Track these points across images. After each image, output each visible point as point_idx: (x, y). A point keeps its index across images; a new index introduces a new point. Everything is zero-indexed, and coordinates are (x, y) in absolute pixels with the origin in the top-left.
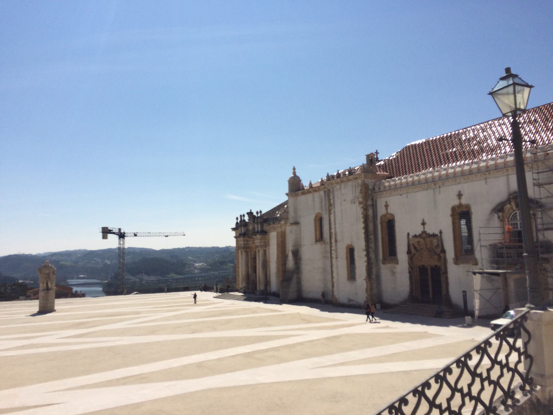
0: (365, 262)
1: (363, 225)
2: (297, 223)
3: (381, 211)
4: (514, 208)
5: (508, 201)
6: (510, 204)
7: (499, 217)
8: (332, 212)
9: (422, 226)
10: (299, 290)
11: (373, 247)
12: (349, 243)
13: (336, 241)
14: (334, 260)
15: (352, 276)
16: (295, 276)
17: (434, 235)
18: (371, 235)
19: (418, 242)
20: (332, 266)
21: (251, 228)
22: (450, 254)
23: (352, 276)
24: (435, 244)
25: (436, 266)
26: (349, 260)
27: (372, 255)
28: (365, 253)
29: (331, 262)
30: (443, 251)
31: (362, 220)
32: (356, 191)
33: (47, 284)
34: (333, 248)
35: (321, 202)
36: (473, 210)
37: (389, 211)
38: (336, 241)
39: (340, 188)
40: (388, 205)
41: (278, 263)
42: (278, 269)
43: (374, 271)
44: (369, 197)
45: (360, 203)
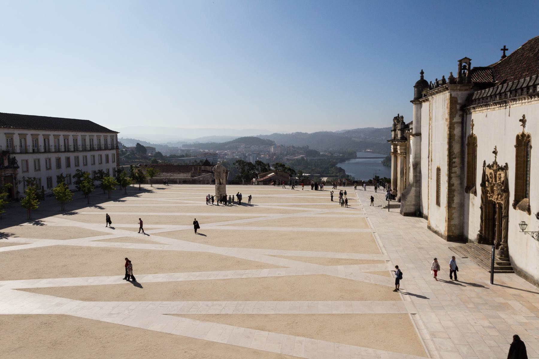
1: (446, 146)
9: (494, 155)
16: (413, 189)
18: (455, 158)
19: (491, 174)
24: (502, 179)
33: (219, 180)
36: (533, 143)
43: (456, 199)
44: (460, 112)
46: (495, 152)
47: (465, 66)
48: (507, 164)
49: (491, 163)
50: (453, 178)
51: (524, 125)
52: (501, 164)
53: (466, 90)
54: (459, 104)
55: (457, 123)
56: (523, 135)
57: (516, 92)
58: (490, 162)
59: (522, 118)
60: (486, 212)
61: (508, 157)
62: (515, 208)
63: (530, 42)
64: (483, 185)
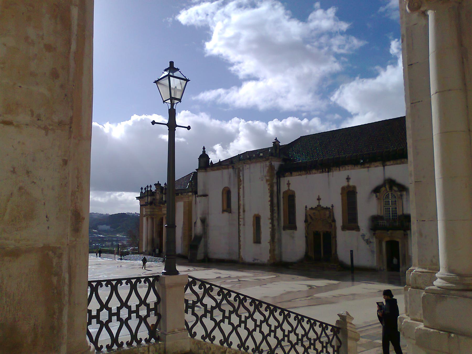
0: (270, 228)
1: (269, 199)
2: (205, 196)
3: (284, 188)
4: (388, 190)
5: (384, 185)
6: (385, 187)
7: (377, 196)
8: (241, 187)
9: (318, 201)
11: (277, 217)
12: (256, 213)
13: (244, 211)
15: (257, 240)
16: (203, 239)
17: (327, 208)
19: (314, 213)
20: (239, 232)
21: (158, 197)
22: (339, 222)
23: (257, 240)
25: (327, 232)
26: (255, 227)
27: (276, 223)
28: (270, 221)
29: (239, 228)
30: (334, 221)
31: (269, 194)
32: (264, 171)
34: (241, 217)
35: (230, 178)
36: (358, 190)
37: (291, 188)
38: (244, 211)
39: (250, 168)
40: (290, 184)
41: (184, 229)
42: (184, 234)
45: (267, 181)
51: (348, 181)
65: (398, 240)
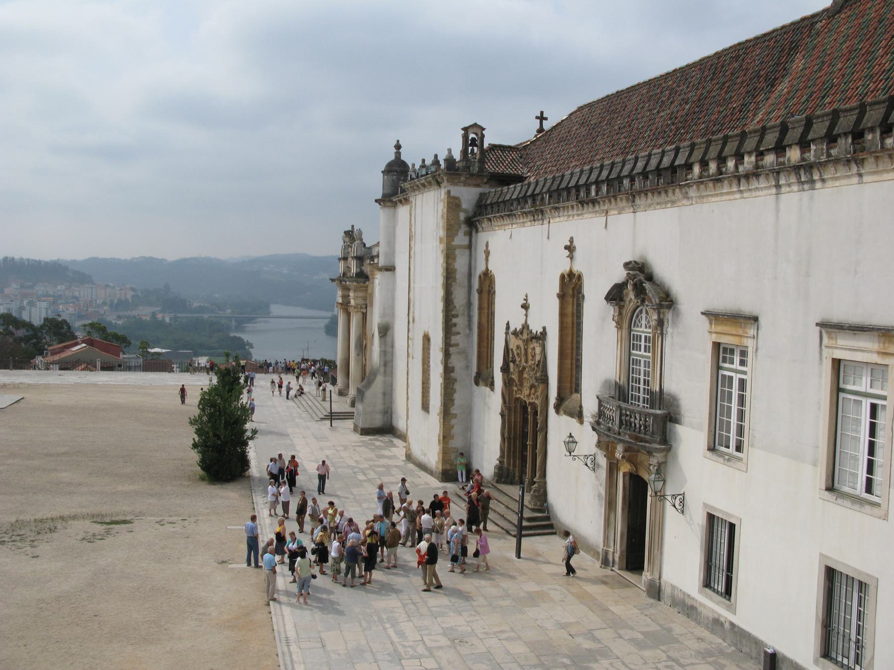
1: (441, 293)
9: (524, 311)
10: (388, 411)
14: (410, 358)
16: (379, 379)
18: (457, 316)
24: (538, 358)
30: (545, 380)
43: (458, 398)
46: (525, 307)
47: (473, 139)
48: (544, 328)
49: (519, 327)
50: (452, 357)
51: (571, 257)
52: (536, 328)
53: (478, 186)
54: (465, 211)
55: (460, 247)
56: (571, 274)
57: (559, 195)
58: (516, 325)
59: (569, 244)
60: (509, 423)
61: (546, 317)
62: (557, 412)
63: (581, 109)
64: (505, 369)
65: (646, 477)
